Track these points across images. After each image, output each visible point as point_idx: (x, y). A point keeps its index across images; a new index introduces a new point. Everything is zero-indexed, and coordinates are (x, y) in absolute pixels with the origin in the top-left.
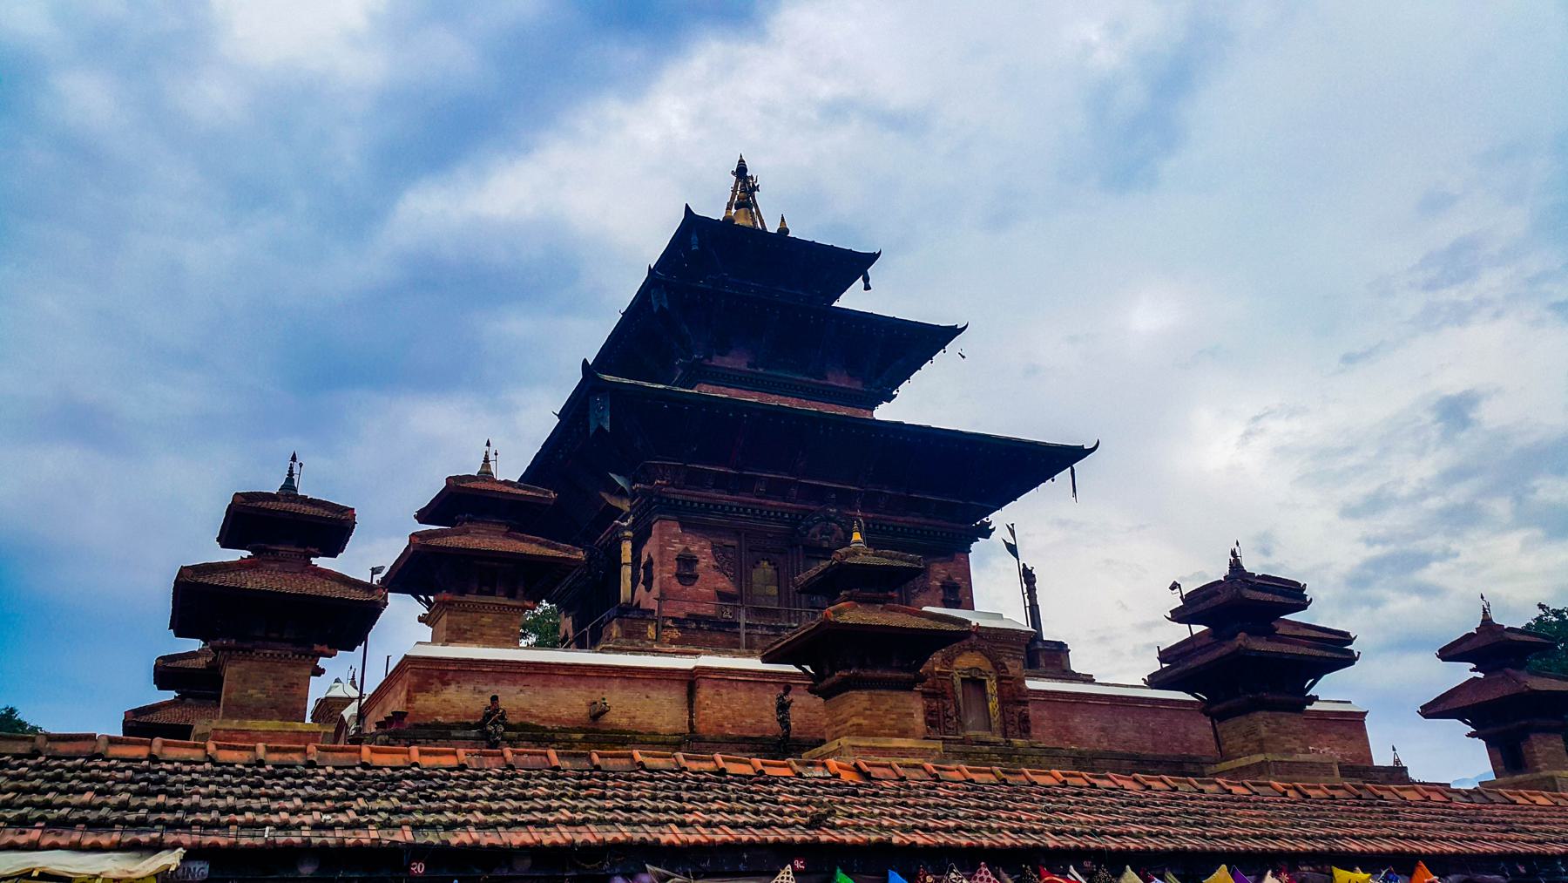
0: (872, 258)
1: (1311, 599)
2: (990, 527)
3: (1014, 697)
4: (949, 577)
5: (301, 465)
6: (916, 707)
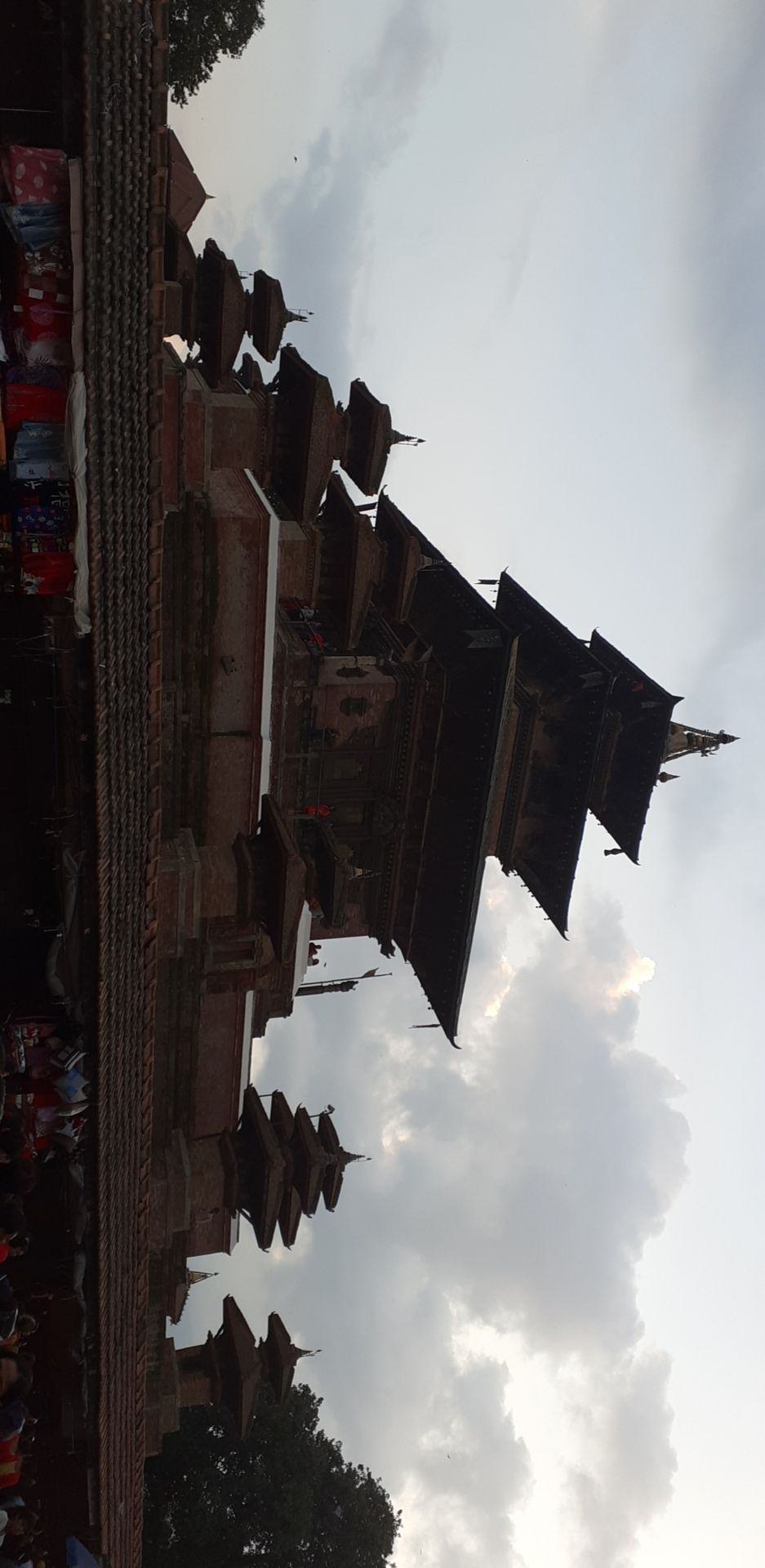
0: (634, 857)
1: (310, 1217)
2: (390, 955)
3: (239, 983)
4: (348, 919)
5: (416, 445)
6: (229, 910)
